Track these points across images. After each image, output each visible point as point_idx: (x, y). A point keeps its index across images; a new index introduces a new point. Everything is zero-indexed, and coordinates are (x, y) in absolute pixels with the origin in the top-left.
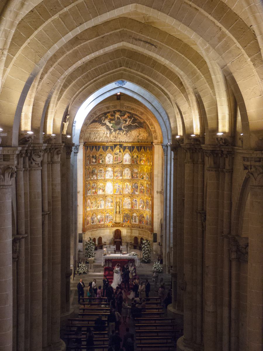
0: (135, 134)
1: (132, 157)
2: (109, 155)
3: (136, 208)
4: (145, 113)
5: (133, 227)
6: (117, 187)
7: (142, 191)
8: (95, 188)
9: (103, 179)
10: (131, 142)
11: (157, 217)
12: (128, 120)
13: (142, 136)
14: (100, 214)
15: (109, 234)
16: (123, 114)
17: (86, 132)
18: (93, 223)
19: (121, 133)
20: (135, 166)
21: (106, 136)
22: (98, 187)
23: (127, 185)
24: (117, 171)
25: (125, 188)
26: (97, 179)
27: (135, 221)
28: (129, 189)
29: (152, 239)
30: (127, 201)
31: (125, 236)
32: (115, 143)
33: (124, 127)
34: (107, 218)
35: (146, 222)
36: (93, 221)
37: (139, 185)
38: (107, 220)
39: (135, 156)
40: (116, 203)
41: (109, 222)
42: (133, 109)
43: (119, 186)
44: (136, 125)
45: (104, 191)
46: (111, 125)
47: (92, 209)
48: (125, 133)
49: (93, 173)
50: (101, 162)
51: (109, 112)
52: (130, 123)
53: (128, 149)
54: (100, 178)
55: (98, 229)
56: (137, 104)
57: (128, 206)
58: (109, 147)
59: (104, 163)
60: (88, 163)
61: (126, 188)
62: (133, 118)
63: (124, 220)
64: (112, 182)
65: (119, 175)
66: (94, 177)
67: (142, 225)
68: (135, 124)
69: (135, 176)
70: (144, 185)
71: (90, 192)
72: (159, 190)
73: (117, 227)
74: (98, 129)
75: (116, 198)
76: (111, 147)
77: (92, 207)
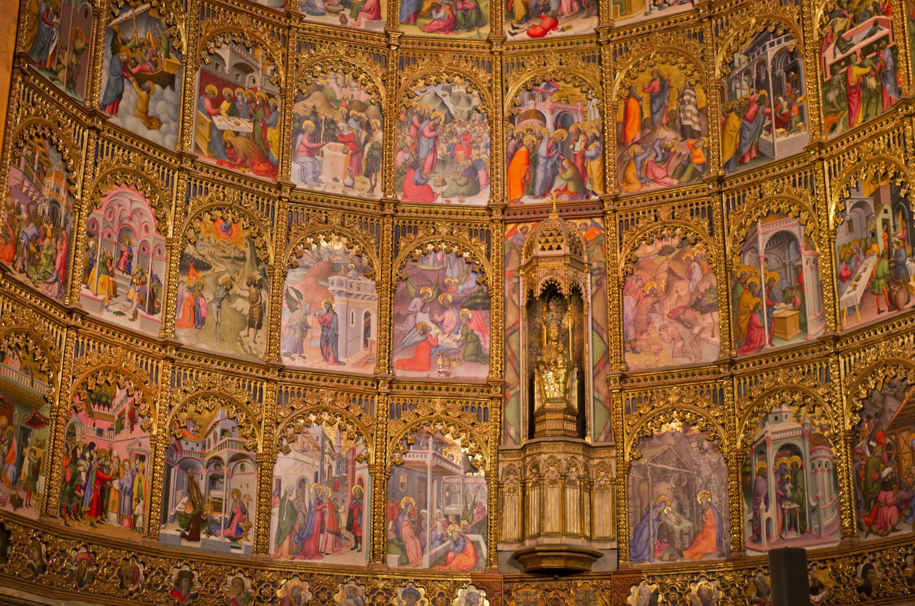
3: (795, 340)
6: (534, 123)
7: (862, 84)
23: (665, 85)
25: (634, 133)
28: (686, 133)
36: (196, 500)
40: (531, 304)
41: (442, 560)
43: (562, 121)
47: (185, 337)
54: (335, 20)
61: (643, 126)
64: (482, 74)
75: (530, 247)
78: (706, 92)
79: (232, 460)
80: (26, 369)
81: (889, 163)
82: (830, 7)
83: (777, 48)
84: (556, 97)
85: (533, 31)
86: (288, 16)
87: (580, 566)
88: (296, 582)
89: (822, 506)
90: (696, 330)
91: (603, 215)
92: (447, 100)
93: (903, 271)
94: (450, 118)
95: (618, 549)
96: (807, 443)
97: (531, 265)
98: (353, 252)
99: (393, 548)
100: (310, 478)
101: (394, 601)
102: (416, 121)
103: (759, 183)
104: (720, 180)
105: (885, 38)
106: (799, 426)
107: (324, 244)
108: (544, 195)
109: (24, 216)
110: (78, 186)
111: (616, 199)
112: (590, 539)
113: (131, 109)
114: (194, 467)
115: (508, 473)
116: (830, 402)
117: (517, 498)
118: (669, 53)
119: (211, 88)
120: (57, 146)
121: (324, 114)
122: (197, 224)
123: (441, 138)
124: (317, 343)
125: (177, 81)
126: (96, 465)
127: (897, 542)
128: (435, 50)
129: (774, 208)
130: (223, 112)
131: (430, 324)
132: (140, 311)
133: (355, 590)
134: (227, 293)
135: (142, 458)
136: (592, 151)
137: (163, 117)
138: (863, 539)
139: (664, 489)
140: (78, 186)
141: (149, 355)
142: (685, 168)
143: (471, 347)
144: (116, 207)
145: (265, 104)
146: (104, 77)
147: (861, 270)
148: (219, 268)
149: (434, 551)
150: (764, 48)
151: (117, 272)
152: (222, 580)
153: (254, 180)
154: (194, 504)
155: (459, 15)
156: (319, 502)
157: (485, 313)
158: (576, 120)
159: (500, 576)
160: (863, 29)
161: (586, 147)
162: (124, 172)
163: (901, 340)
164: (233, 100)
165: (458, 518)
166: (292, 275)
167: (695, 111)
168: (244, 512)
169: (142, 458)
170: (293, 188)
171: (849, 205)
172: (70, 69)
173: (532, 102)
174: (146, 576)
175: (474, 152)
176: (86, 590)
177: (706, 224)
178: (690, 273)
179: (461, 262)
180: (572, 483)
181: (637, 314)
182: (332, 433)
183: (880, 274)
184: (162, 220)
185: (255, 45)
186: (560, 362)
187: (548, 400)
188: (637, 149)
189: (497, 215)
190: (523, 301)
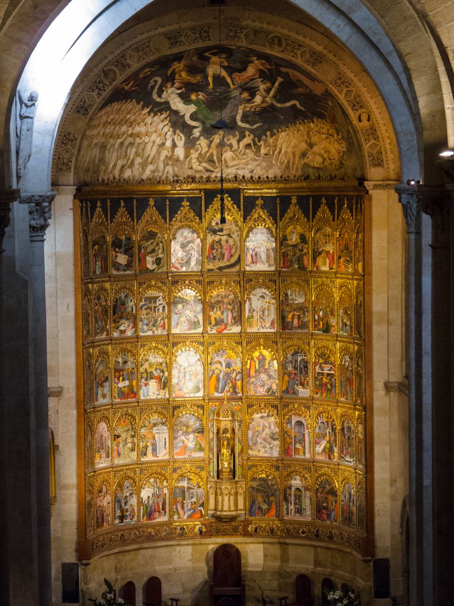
0: (292, 144)
1: (281, 244)
2: (185, 234)
3: (302, 457)
4: (331, 56)
5: (289, 534)
6: (218, 366)
7: (326, 386)
8: (130, 375)
9: (161, 336)
10: (275, 180)
11: (388, 490)
12: (262, 87)
13: (321, 155)
14: (152, 480)
15: (190, 564)
16: (237, 66)
17: (85, 143)
18: (122, 518)
19: (234, 141)
20: (294, 279)
22: (142, 370)
23: (264, 358)
24: (219, 302)
25: (253, 373)
26: (138, 337)
27: (299, 511)
28: (270, 377)
29: (371, 583)
30: (264, 427)
31: (260, 572)
32: (209, 186)
33: (245, 118)
34: (180, 499)
35: (343, 511)
36: (122, 511)
37: (312, 358)
38: (179, 508)
39: (294, 239)
41: (190, 516)
42: (278, 41)
43: (228, 365)
44: (294, 106)
45: (165, 384)
46: (192, 108)
47: (117, 461)
48: (247, 140)
49: (118, 311)
50: (150, 266)
51: (178, 57)
52: (268, 99)
54: (150, 333)
55: (145, 545)
56: (293, 20)
57: (268, 446)
58: (186, 203)
59: (165, 269)
60: (98, 272)
61: (256, 372)
62: (280, 80)
63: (251, 507)
64: (201, 347)
65: (228, 317)
66: (122, 328)
68: (288, 104)
69: (293, 319)
70: (333, 359)
71: (106, 390)
72: (396, 377)
73: (225, 534)
74: (137, 129)
75: (218, 415)
76: (195, 203)
77: (115, 454)
83: (301, 358)
84: (226, 356)
88: (150, 530)
90: (272, 446)
91: (242, 402)
99: (176, 514)
100: (151, 496)
105: (333, 374)
106: (300, 483)
108: (222, 393)
111: (247, 398)
117: (214, 496)
118: (266, 348)
119: (117, 374)
123: (187, 372)
124: (151, 451)
131: (185, 439)
134: (126, 444)
135: (109, 503)
136: (238, 377)
143: (198, 446)
145: (132, 372)
156: (154, 503)
160: (328, 367)
161: (236, 376)
164: (123, 375)
165: (195, 503)
166: (143, 430)
168: (133, 510)
173: (217, 358)
175: (198, 376)
178: (270, 427)
179: (194, 417)
180: (232, 494)
189: (207, 401)
190: (215, 431)
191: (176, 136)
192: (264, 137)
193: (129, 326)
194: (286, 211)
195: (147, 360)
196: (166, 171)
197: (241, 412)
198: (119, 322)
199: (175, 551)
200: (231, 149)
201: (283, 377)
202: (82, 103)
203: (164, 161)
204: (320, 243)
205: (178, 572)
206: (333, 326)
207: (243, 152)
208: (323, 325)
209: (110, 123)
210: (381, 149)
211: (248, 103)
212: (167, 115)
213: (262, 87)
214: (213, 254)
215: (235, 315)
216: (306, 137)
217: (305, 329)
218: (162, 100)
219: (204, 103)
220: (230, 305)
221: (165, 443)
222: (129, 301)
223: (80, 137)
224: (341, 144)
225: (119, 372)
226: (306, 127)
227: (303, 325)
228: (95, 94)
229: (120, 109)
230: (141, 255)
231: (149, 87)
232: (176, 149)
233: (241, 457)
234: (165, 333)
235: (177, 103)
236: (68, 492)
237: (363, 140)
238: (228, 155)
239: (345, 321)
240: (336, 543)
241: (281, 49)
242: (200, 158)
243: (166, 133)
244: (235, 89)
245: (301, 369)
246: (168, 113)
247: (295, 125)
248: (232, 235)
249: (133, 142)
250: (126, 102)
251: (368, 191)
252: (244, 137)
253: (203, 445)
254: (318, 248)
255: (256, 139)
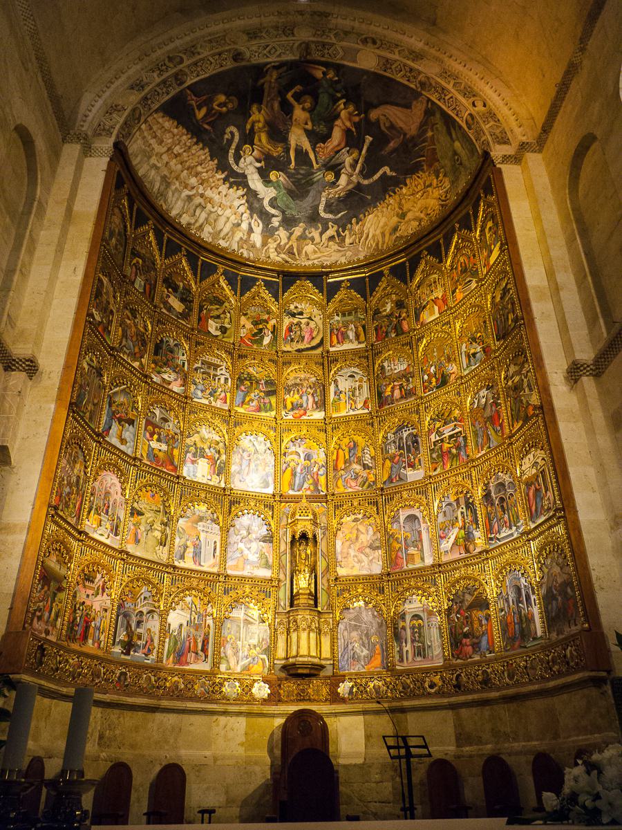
0: (381, 224)
3: (418, 565)
5: (408, 693)
6: (295, 457)
7: (450, 452)
8: (171, 440)
15: (241, 751)
18: (129, 646)
19: (315, 234)
21: (246, 241)
22: (188, 441)
23: (356, 445)
25: (341, 465)
26: (186, 398)
27: (421, 652)
28: (365, 467)
31: (361, 767)
33: (329, 208)
36: (130, 634)
39: (388, 308)
41: (247, 668)
43: (308, 457)
45: (221, 469)
47: (131, 548)
48: (331, 232)
49: (162, 354)
53: (348, 288)
54: (206, 402)
61: (345, 462)
62: (369, 139)
64: (272, 433)
67: (478, 663)
68: (376, 177)
69: (392, 392)
70: (457, 413)
72: (586, 354)
73: (302, 697)
75: (293, 514)
77: (130, 537)
78: (374, 449)
79: (148, 613)
80: (58, 561)
81: (463, 487)
82: (433, 417)
83: (408, 432)
85: (296, 416)
86: (186, 398)
87: (316, 673)
89: (433, 645)
92: (255, 443)
93: (471, 536)
94: (256, 451)
95: (333, 664)
96: (425, 614)
97: (294, 523)
98: (210, 511)
100: (185, 624)
101: (224, 689)
102: (241, 453)
103: (401, 492)
104: (382, 489)
105: (460, 432)
107: (196, 506)
108: (299, 491)
109: (66, 482)
110: (89, 469)
111: (333, 495)
112: (320, 658)
113: (114, 435)
114: (130, 616)
115: (280, 624)
116: (436, 595)
117: (284, 637)
119: (150, 428)
120: (82, 449)
121: (199, 445)
122: (139, 493)
124: (191, 555)
125: (135, 423)
126: (84, 613)
127: (475, 663)
128: (251, 420)
129: (407, 503)
130: (154, 440)
132: (111, 534)
133: (205, 683)
135: (106, 610)
136: (321, 472)
137: (128, 440)
138: (454, 662)
139: (354, 634)
140: (89, 469)
141: (113, 557)
142: (365, 483)
143: (264, 561)
144: (104, 481)
145: (173, 437)
146: (104, 419)
147: (451, 534)
148: (148, 515)
149: (243, 663)
150: (402, 432)
151: (102, 513)
152: (141, 677)
153: (167, 473)
154: (129, 636)
155: (262, 405)
156: (189, 636)
157: (271, 544)
158: (314, 457)
159: (276, 677)
160: (450, 427)
161: (319, 470)
162: (109, 464)
163: (472, 567)
164: (159, 434)
166: (181, 521)
167: (370, 457)
168: (152, 640)
169: (106, 610)
170: (184, 478)
171: (444, 504)
172: (90, 413)
174: (104, 674)
175: (267, 468)
176: (76, 682)
177: (375, 509)
178: (367, 531)
180: (312, 630)
181: (342, 549)
182: (197, 602)
183: (460, 536)
184: (124, 490)
185: (171, 410)
186: (306, 570)
187: (300, 589)
188: (343, 472)
189: (277, 498)
190: (289, 540)
191: (253, 220)
192: (349, 226)
193: (176, 380)
194: (377, 285)
195: (198, 432)
196: (241, 251)
197: (325, 515)
198: (161, 367)
199: (218, 725)
200: (313, 242)
201: (383, 465)
202: (138, 82)
203: (238, 243)
204: (424, 296)
205: (218, 763)
206: (453, 373)
207: (326, 245)
208: (436, 382)
209: (176, 156)
210: (504, 129)
211: (333, 188)
212: (244, 193)
213: (348, 160)
214: (290, 336)
215: (316, 400)
216: (397, 209)
217: (411, 397)
218: (240, 171)
219: (285, 188)
220: (311, 388)
221: (215, 549)
222: (180, 354)
223: (130, 108)
224: (441, 186)
225: (153, 428)
226: (397, 196)
227: (409, 394)
228: (155, 75)
229: (190, 148)
230: (201, 315)
231: (225, 140)
232: (252, 235)
233: (325, 578)
234: (227, 408)
235: (256, 181)
236: (10, 538)
237: (481, 122)
238: (309, 248)
239: (472, 351)
240: (499, 689)
241: (377, 46)
242: (279, 249)
243: (242, 214)
244: (319, 169)
245: (408, 447)
246: (245, 190)
247: (384, 201)
248: (313, 318)
249: (203, 204)
250: (196, 143)
251: (495, 166)
252: (328, 228)
253: (271, 561)
254: (421, 303)
255: (340, 230)
